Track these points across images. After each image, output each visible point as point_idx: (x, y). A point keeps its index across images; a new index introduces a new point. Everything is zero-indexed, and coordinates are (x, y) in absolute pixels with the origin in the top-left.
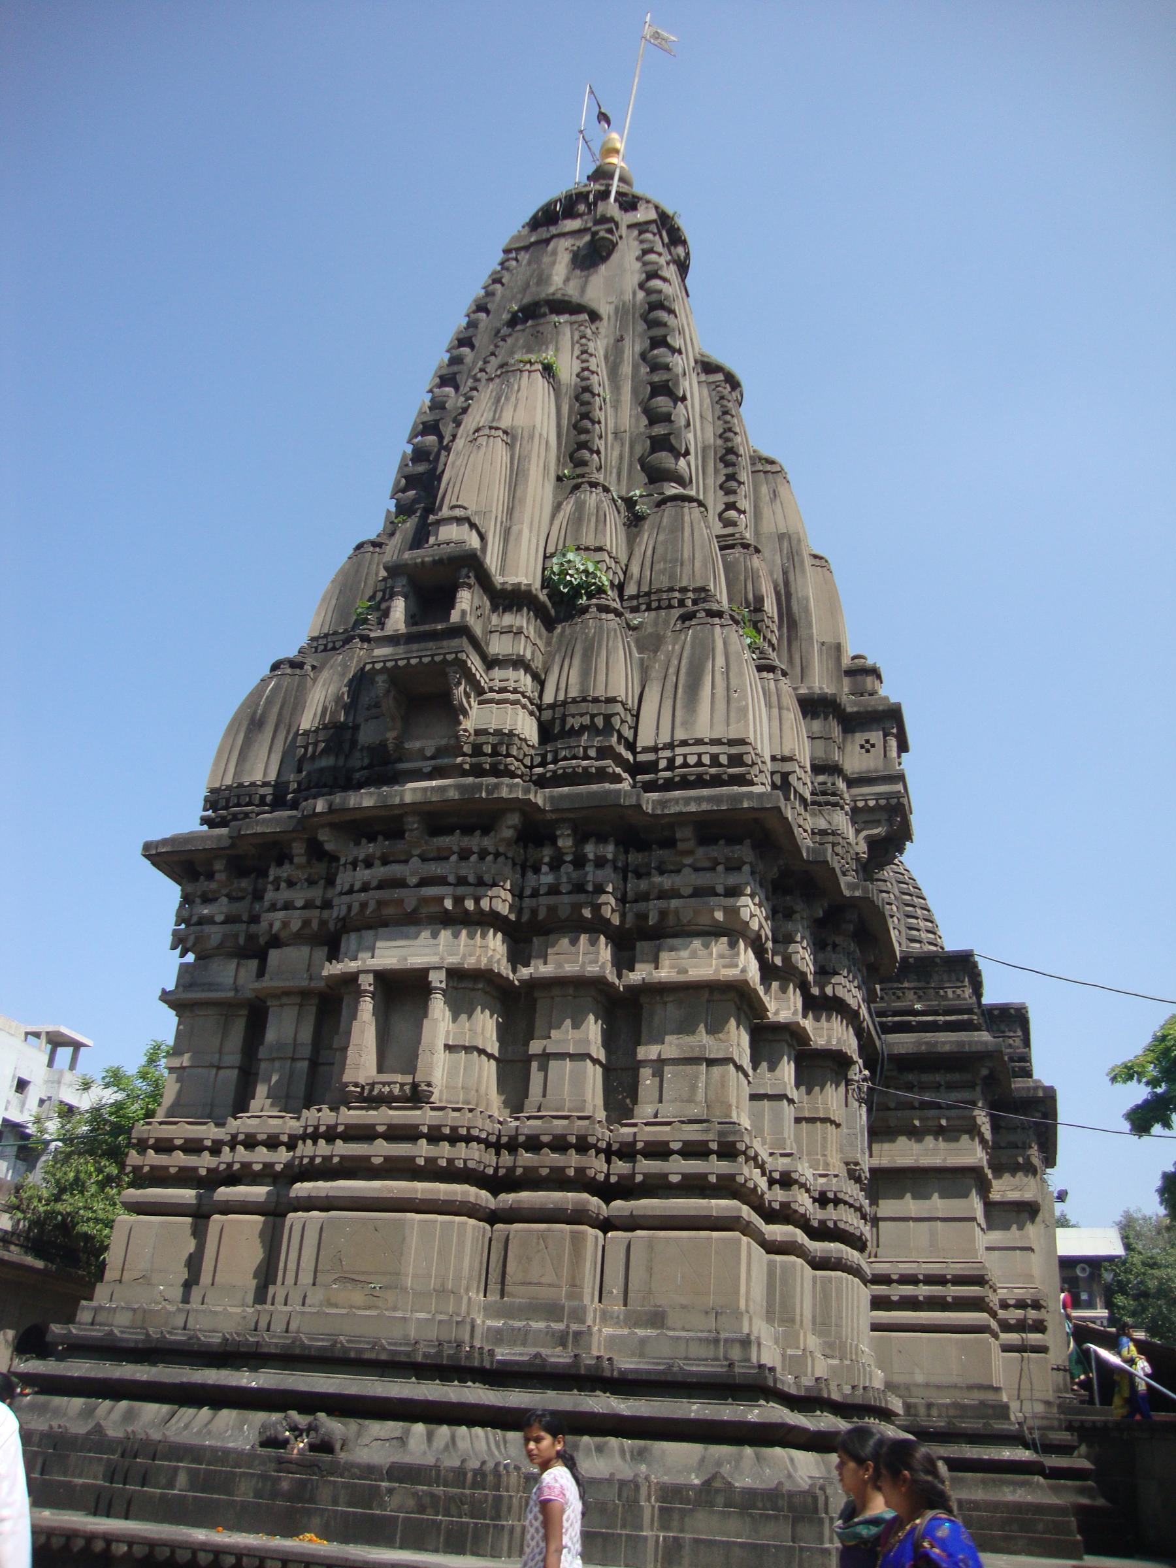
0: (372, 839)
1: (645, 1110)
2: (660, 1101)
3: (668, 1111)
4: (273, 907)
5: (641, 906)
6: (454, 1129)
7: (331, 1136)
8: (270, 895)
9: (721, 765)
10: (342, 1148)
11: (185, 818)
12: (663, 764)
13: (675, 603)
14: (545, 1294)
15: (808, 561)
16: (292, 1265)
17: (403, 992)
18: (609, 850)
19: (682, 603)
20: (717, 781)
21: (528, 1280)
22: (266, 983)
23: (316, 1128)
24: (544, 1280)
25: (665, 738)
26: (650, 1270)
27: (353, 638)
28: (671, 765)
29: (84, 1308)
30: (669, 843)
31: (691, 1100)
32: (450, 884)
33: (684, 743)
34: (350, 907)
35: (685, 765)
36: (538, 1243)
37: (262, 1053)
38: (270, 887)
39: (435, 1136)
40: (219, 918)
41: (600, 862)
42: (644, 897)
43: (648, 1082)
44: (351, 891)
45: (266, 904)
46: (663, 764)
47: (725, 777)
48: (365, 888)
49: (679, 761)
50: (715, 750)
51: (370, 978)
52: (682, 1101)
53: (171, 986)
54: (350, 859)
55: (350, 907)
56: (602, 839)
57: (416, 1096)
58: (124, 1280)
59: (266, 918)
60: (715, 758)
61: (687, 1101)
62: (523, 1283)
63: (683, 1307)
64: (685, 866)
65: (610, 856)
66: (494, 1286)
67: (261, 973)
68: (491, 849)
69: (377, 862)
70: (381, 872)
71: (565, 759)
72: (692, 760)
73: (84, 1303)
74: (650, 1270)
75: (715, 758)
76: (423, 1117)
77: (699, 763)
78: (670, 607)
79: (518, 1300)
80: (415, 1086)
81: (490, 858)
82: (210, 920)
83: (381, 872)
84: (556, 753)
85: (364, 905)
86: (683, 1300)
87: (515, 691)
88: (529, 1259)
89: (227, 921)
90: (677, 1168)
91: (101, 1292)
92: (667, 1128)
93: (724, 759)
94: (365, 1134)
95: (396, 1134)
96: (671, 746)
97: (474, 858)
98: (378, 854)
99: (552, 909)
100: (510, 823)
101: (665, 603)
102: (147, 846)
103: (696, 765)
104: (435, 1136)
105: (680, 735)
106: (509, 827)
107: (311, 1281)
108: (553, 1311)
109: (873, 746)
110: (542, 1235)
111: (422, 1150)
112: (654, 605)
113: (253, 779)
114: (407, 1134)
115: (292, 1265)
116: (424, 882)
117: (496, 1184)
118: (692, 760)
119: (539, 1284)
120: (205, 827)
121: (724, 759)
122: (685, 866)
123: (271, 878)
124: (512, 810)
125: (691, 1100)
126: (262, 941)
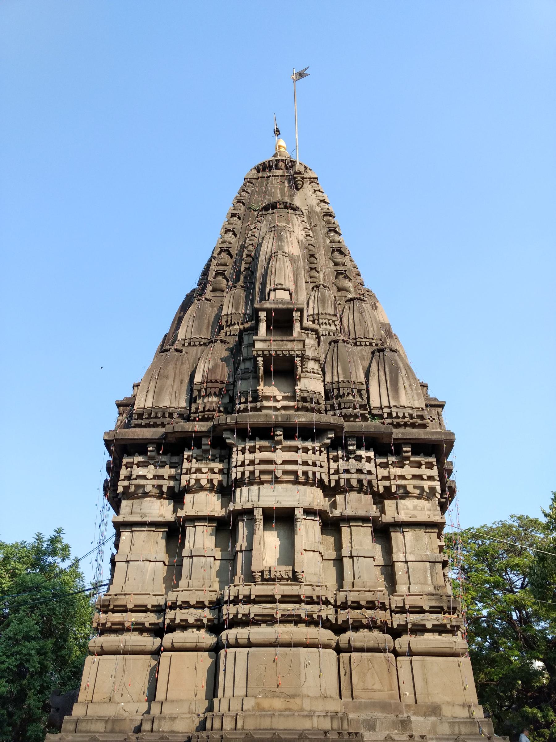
1: (402, 588)
2: (410, 584)
3: (415, 589)
4: (189, 472)
6: (318, 598)
7: (248, 600)
8: (186, 465)
10: (256, 609)
12: (385, 416)
14: (379, 696)
15: (269, 348)
16: (229, 684)
17: (282, 519)
18: (371, 454)
20: (413, 426)
21: (366, 688)
22: (181, 513)
24: (375, 687)
25: (385, 403)
26: (425, 680)
27: (216, 341)
28: (390, 415)
29: (68, 722)
30: (398, 452)
31: (425, 583)
32: (300, 465)
33: (396, 407)
35: (397, 417)
36: (368, 664)
39: (310, 601)
40: (150, 476)
41: (369, 459)
43: (400, 573)
45: (184, 471)
46: (385, 416)
47: (417, 424)
48: (252, 463)
49: (394, 415)
50: (410, 411)
51: (261, 512)
52: (421, 584)
55: (243, 474)
57: (295, 578)
58: (94, 700)
59: (185, 478)
61: (423, 584)
62: (364, 690)
63: (448, 703)
64: (406, 464)
65: (373, 457)
66: (346, 692)
68: (318, 448)
69: (257, 451)
70: (259, 456)
71: (345, 408)
72: (401, 415)
73: (66, 718)
74: (425, 680)
76: (303, 591)
77: (404, 417)
79: (363, 700)
80: (294, 572)
81: (318, 453)
82: (144, 477)
83: (259, 456)
84: (340, 405)
86: (447, 699)
88: (365, 675)
89: (156, 477)
90: (430, 620)
91: (78, 710)
94: (271, 599)
95: (286, 599)
96: (389, 407)
97: (310, 452)
99: (348, 481)
100: (330, 436)
101: (363, 344)
104: (310, 601)
105: (393, 403)
107: (244, 693)
108: (384, 707)
109: (434, 419)
110: (370, 660)
111: (304, 610)
112: (358, 344)
113: (165, 405)
114: (297, 600)
115: (229, 684)
116: (285, 462)
117: (338, 629)
119: (373, 690)
122: (406, 464)
124: (331, 430)
125: (425, 583)
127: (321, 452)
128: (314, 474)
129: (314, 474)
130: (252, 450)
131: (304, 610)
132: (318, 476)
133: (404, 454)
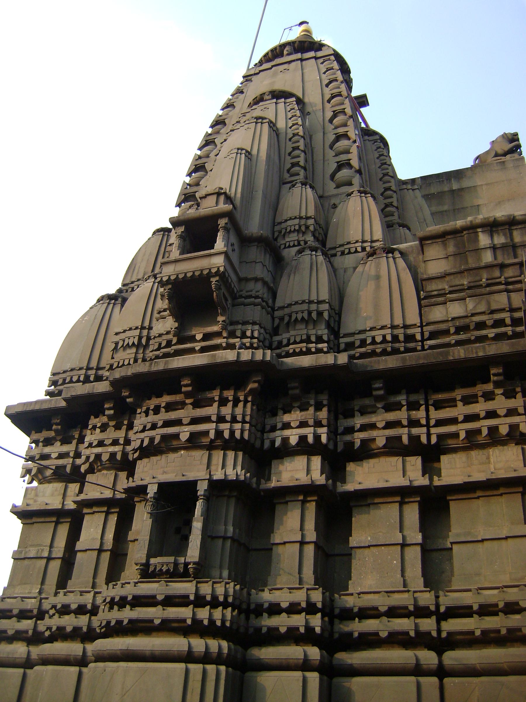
0: (159, 396)
5: (348, 438)
9: (399, 342)
11: (34, 389)
13: (359, 249)
19: (364, 249)
23: (113, 599)
34: (142, 441)
37: (79, 546)
38: (89, 432)
42: (351, 430)
44: (143, 431)
49: (369, 341)
53: (19, 502)
54: (144, 409)
56: (319, 392)
60: (395, 338)
67: (81, 491)
68: (242, 398)
70: (164, 416)
72: (379, 339)
75: (395, 338)
77: (384, 340)
78: (356, 251)
81: (241, 405)
85: (152, 439)
87: (257, 297)
92: (376, 596)
93: (401, 338)
98: (163, 405)
101: (353, 250)
102: (8, 408)
103: (381, 343)
106: (255, 382)
118: (379, 339)
120: (48, 397)
121: (401, 338)
123: (90, 427)
126: (83, 469)
127: (246, 402)
128: (232, 432)
129: (232, 432)
130: (157, 410)
131: (185, 613)
132: (238, 435)
133: (375, 393)
